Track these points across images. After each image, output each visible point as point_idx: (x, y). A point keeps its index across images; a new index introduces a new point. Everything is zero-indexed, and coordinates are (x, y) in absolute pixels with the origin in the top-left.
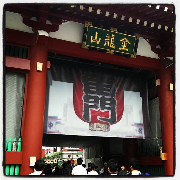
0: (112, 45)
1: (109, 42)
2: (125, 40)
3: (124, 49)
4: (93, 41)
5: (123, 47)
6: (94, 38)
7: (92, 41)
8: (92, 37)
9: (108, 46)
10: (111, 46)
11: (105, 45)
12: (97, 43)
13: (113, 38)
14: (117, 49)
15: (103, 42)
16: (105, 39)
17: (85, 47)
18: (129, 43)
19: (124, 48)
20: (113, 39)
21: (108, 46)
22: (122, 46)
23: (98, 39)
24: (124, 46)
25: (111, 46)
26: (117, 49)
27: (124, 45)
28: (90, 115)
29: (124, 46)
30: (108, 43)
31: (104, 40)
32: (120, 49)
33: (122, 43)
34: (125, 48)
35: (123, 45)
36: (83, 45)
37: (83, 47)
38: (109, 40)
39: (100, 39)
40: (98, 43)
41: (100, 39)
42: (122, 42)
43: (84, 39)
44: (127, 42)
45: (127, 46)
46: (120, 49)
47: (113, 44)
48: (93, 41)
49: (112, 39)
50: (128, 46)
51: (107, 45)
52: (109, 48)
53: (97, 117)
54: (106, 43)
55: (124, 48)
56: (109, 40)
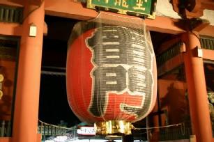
3: (139, 8)
11: (116, 4)
14: (130, 8)
17: (91, 7)
22: (137, 5)
24: (140, 5)
25: (123, 5)
26: (130, 8)
28: (107, 102)
32: (135, 8)
46: (135, 8)
51: (118, 4)
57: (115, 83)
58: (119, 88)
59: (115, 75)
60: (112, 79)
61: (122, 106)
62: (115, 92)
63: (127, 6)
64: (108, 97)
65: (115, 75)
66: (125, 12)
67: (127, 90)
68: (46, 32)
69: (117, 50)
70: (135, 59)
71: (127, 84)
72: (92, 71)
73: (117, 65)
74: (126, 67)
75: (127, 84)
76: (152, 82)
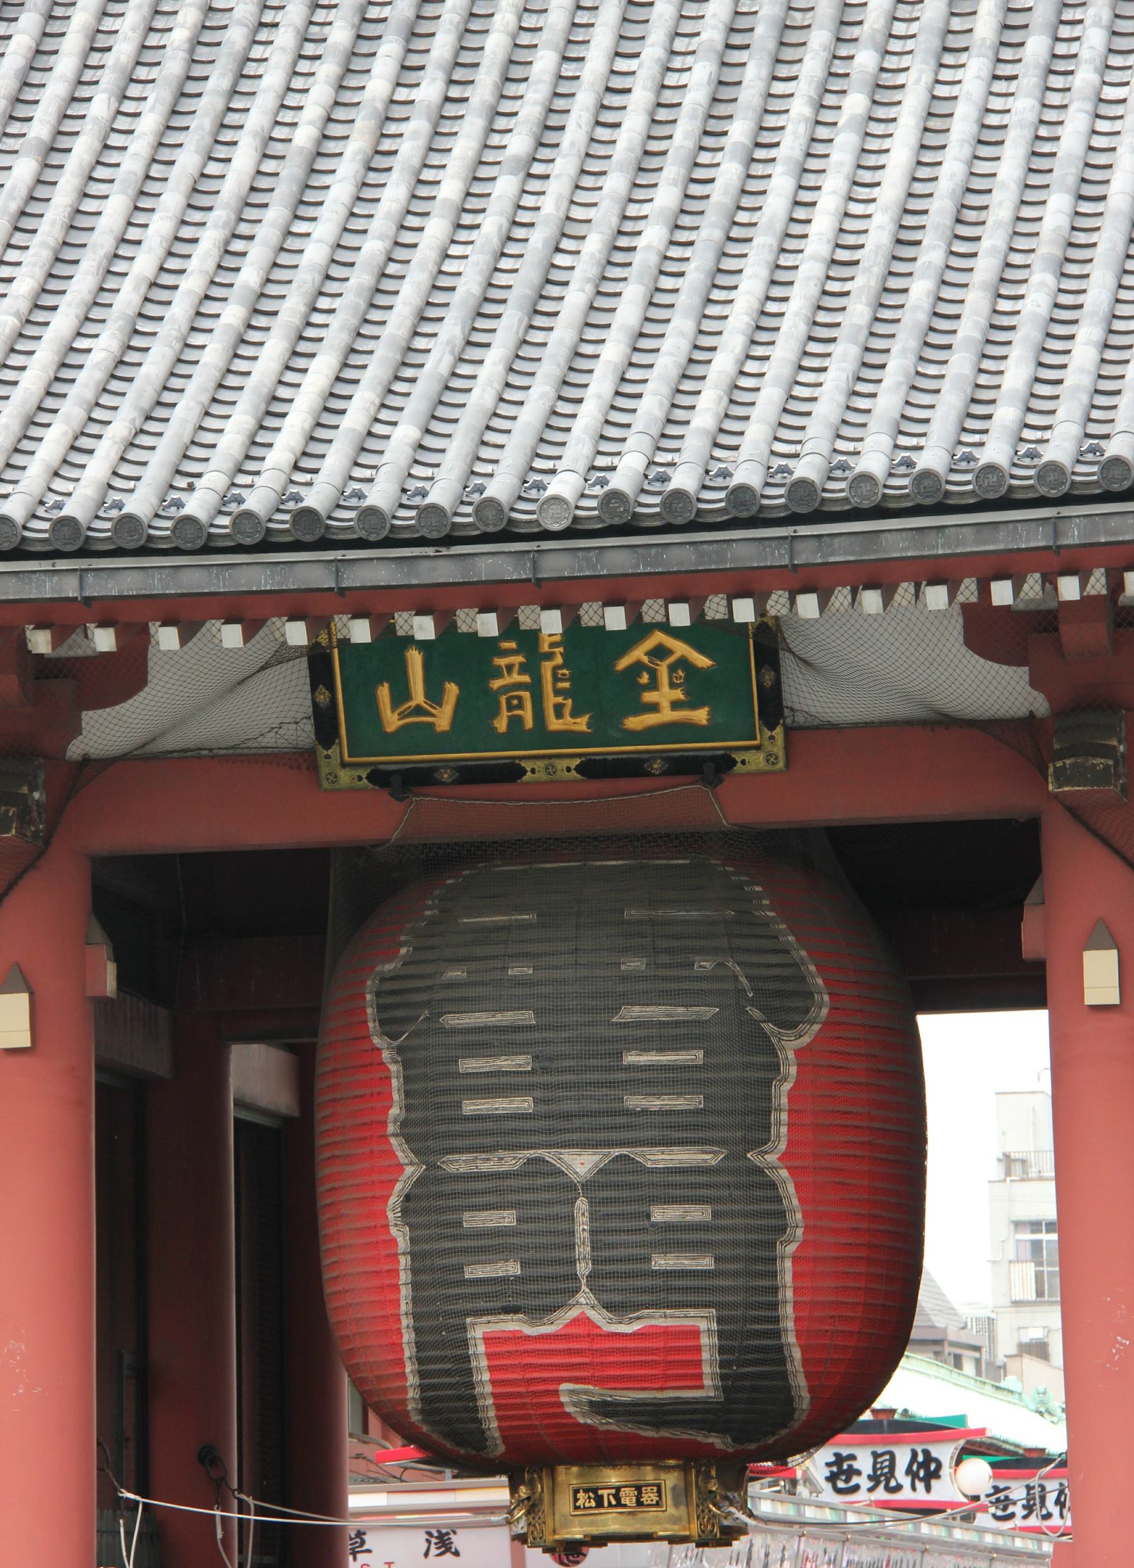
0: (559, 711)
1: (526, 695)
2: (660, 652)
3: (667, 715)
4: (402, 716)
5: (654, 708)
6: (401, 694)
7: (392, 721)
8: (384, 693)
9: (529, 723)
10: (555, 724)
11: (501, 724)
12: (431, 725)
13: (559, 660)
15: (477, 706)
16: (496, 684)
18: (702, 661)
19: (665, 705)
20: (555, 669)
21: (529, 723)
22: (649, 697)
23: (435, 694)
24: (665, 694)
26: (606, 725)
27: (665, 688)
29: (665, 694)
30: (520, 706)
31: (487, 692)
32: (634, 723)
33: (645, 679)
34: (676, 705)
35: (654, 685)
36: (324, 770)
37: (326, 785)
38: (526, 679)
39: (452, 690)
40: (443, 719)
41: (452, 690)
42: (638, 667)
43: (324, 723)
44: (683, 663)
45: (687, 693)
46: (634, 723)
47: (569, 702)
48: (402, 716)
49: (547, 667)
50: (697, 688)
52: (542, 736)
53: (556, 1393)
54: (510, 708)
55: (665, 705)
56: (526, 679)
57: (513, 1269)
58: (542, 1291)
59: (507, 1219)
60: (493, 1244)
61: (572, 1396)
62: (512, 1324)
63: (581, 724)
64: (481, 1349)
65: (507, 1219)
66: (566, 767)
67: (585, 1305)
68: (109, 982)
69: (521, 1062)
70: (635, 1102)
71: (583, 1269)
72: (392, 1200)
73: (510, 1161)
74: (581, 1164)
75: (583, 1269)
76: (783, 1229)
